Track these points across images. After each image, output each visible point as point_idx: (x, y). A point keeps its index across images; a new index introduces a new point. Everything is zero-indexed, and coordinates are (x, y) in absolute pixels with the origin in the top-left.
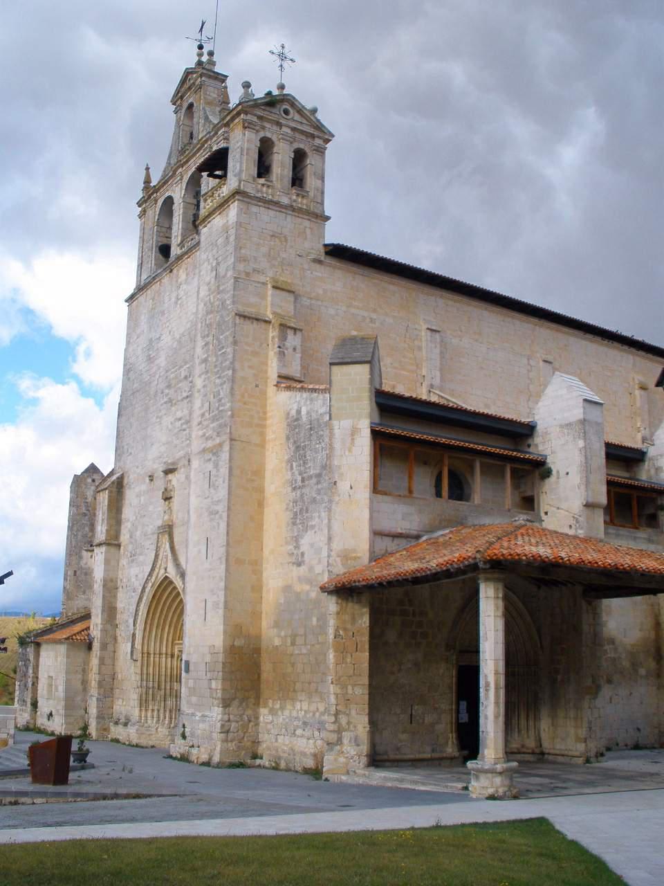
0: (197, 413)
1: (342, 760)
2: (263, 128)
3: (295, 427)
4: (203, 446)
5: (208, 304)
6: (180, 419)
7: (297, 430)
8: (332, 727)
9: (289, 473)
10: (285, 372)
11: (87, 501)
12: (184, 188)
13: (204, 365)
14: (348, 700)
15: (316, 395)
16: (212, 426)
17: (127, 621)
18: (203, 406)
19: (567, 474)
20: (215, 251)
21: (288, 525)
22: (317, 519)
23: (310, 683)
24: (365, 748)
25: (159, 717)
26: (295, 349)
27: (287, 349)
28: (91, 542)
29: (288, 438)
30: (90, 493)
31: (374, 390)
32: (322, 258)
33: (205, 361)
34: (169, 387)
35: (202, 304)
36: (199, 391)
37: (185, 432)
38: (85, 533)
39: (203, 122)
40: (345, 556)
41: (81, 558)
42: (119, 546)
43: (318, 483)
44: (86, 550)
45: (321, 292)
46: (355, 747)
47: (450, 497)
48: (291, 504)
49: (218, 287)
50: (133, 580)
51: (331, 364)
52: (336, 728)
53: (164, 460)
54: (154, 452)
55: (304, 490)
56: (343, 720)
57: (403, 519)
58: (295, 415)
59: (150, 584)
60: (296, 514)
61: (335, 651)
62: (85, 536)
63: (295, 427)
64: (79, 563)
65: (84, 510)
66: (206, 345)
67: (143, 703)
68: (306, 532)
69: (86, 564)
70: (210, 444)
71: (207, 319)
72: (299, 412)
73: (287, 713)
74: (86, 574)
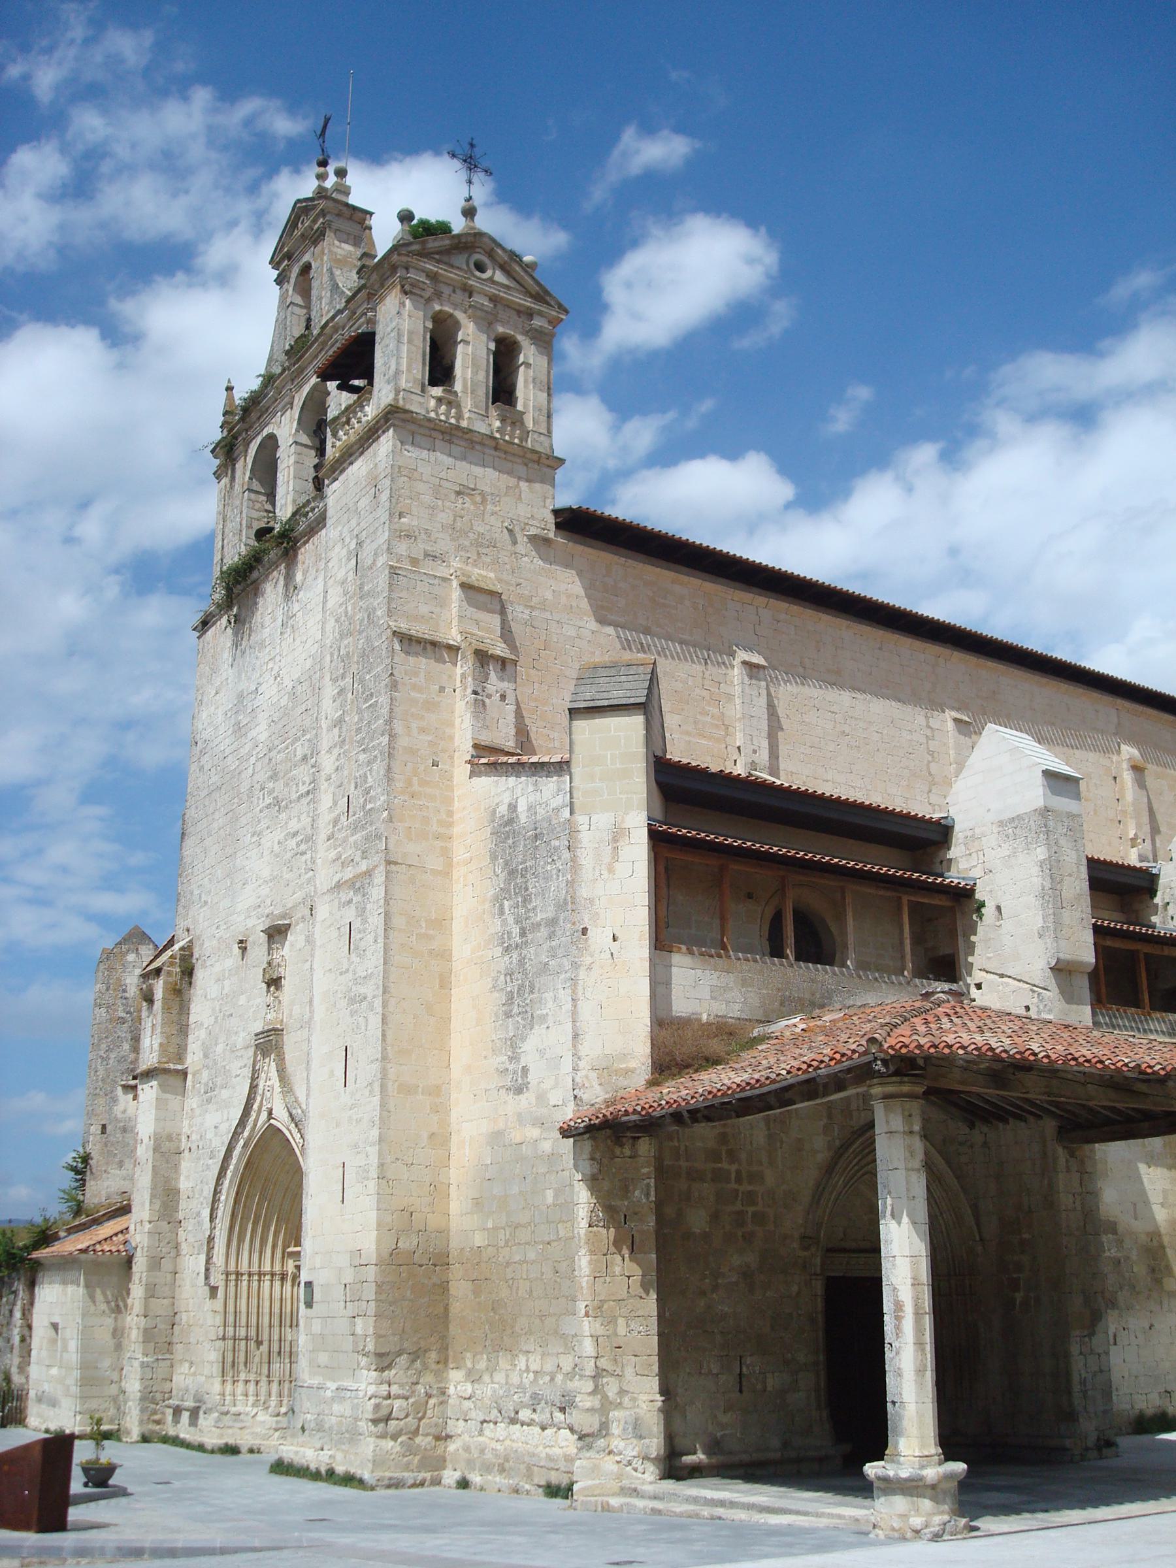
0: (325, 819)
2: (438, 295)
4: (337, 878)
7: (510, 841)
8: (589, 1402)
9: (498, 922)
10: (486, 738)
11: (127, 995)
12: (297, 417)
13: (336, 730)
14: (620, 1347)
16: (352, 839)
17: (198, 1214)
18: (335, 803)
20: (353, 523)
22: (550, 1004)
24: (655, 1445)
26: (503, 697)
27: (489, 696)
29: (494, 857)
31: (652, 760)
32: (551, 535)
33: (339, 722)
34: (274, 777)
35: (333, 620)
36: (328, 779)
37: (304, 858)
39: (328, 294)
40: (606, 1070)
41: (115, 1100)
42: (184, 1073)
45: (549, 595)
46: (635, 1441)
47: (798, 959)
48: (502, 977)
50: (209, 1135)
51: (574, 713)
52: (597, 1404)
53: (267, 911)
54: (247, 898)
55: (524, 952)
56: (612, 1391)
57: (713, 998)
59: (242, 1142)
60: (510, 997)
61: (592, 1252)
66: (340, 693)
67: (228, 1368)
69: (124, 1111)
70: (349, 873)
71: (342, 646)
72: (513, 807)
73: (499, 1377)
74: (124, 1130)
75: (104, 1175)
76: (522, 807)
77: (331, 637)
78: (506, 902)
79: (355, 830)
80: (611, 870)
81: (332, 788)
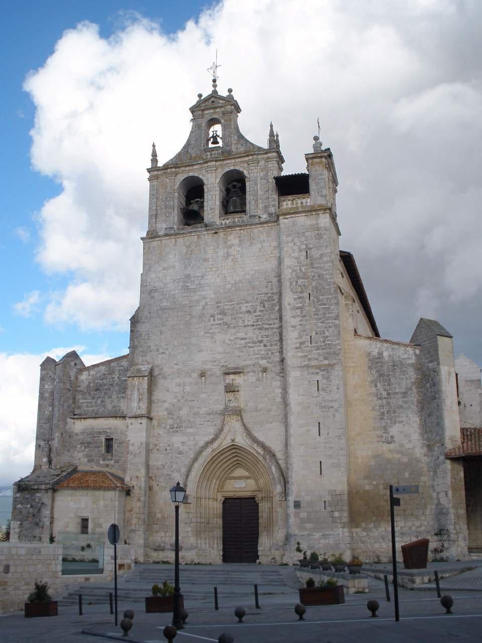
1: (460, 549)
3: (378, 362)
4: (306, 363)
5: (298, 271)
6: (242, 339)
7: (380, 364)
11: (71, 379)
13: (299, 311)
15: (397, 347)
18: (300, 337)
19: (471, 405)
20: (303, 239)
21: (375, 419)
23: (405, 511)
28: (73, 411)
29: (370, 368)
30: (73, 374)
35: (290, 271)
37: (252, 349)
38: (69, 404)
39: (236, 137)
41: (66, 423)
43: (403, 397)
44: (71, 418)
48: (378, 407)
49: (312, 264)
53: (221, 364)
56: (458, 527)
58: (377, 355)
60: (383, 414)
61: (452, 490)
62: (69, 407)
63: (378, 362)
64: (65, 427)
65: (68, 386)
67: (198, 534)
68: (395, 424)
69: (70, 429)
71: (299, 281)
74: (70, 436)
75: (63, 455)
76: (385, 354)
77: (289, 276)
79: (318, 348)
80: (449, 383)
81: (298, 331)
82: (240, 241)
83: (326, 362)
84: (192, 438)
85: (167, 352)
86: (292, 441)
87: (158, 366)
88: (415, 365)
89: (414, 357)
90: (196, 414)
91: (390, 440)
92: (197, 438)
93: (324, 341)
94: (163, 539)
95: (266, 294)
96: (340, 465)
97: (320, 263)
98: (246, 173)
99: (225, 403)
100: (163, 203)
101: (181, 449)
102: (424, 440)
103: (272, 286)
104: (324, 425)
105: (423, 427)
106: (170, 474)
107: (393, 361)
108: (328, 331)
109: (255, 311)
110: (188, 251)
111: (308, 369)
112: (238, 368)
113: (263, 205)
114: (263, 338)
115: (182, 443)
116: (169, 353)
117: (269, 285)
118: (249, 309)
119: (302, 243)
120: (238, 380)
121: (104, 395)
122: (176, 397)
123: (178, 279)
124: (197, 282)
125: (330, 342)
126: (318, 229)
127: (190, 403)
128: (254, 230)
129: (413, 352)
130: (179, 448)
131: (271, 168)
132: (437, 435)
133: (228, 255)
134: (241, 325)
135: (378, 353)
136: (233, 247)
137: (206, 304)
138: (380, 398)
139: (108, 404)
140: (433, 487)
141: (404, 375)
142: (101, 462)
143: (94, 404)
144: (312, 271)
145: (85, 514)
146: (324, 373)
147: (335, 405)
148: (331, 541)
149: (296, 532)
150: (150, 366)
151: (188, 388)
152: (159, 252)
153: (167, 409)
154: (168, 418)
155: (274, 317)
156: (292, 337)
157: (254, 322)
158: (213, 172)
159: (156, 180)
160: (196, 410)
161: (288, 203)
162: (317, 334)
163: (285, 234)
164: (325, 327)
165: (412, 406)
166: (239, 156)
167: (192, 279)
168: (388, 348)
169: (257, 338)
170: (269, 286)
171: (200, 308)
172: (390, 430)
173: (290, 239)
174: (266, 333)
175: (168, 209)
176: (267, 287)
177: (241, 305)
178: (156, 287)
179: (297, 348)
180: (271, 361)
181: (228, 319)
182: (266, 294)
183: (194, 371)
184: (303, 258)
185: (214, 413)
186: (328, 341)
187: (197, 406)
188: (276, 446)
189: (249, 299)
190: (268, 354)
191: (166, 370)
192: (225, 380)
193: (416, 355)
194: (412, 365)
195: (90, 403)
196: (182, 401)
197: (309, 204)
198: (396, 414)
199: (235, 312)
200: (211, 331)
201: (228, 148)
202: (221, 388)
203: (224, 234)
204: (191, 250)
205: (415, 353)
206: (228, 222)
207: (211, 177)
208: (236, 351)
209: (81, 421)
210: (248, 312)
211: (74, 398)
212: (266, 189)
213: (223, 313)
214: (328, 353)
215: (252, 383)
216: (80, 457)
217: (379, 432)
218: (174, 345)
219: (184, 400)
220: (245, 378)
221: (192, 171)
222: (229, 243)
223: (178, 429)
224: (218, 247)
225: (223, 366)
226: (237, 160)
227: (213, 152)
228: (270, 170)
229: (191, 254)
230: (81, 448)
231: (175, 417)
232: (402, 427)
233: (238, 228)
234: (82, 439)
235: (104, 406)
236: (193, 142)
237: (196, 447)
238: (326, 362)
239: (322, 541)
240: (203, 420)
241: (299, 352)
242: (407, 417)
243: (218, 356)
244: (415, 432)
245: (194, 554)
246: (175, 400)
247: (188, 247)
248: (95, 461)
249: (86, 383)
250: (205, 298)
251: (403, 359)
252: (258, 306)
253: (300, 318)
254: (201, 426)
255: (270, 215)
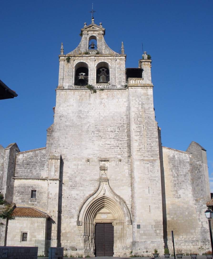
4: (142, 158)
5: (138, 114)
6: (109, 144)
7: (174, 161)
13: (138, 133)
21: (172, 186)
22: (185, 187)
25: (90, 246)
29: (169, 163)
35: (134, 113)
38: (12, 171)
48: (173, 181)
53: (98, 156)
60: (175, 184)
63: (173, 160)
69: (12, 184)
72: (174, 156)
76: (176, 156)
77: (134, 116)
78: (173, 170)
82: (107, 97)
83: (152, 158)
84: (82, 192)
85: (69, 148)
86: (136, 195)
87: (64, 154)
88: (189, 162)
89: (189, 159)
90: (84, 180)
91: (179, 196)
92: (85, 192)
93: (151, 148)
94: (66, 244)
95: (120, 124)
96: (159, 207)
97: (148, 112)
98: (109, 64)
99: (100, 176)
100: (67, 73)
101: (76, 197)
102: (194, 197)
103: (123, 120)
104: (152, 188)
105: (194, 191)
106: (70, 210)
107: (180, 160)
108: (153, 143)
109: (115, 131)
110: (80, 98)
111: (143, 161)
112: (106, 159)
113: (118, 81)
114: (119, 144)
115: (77, 194)
116: (70, 148)
117: (122, 119)
118: (112, 130)
119: (140, 101)
120: (107, 164)
121: (32, 167)
122: (73, 171)
123: (75, 112)
124: (85, 114)
125: (154, 149)
126: (148, 95)
127: (81, 175)
128: (115, 92)
129: (188, 156)
130: (75, 197)
131: (123, 64)
132: (202, 195)
133: (101, 103)
134: (108, 137)
135: (173, 156)
136: (104, 99)
137: (90, 125)
138: (174, 177)
139: (34, 173)
140: (199, 219)
141: (184, 167)
142: (29, 203)
143: (26, 172)
144: (145, 115)
145: (25, 231)
146: (151, 163)
147: (157, 179)
148: (155, 245)
149: (138, 240)
150: (60, 154)
151: (80, 167)
152: (65, 97)
153: (69, 177)
154: (69, 181)
155: (124, 135)
156: (135, 145)
157: (114, 137)
158: (93, 62)
159: (63, 61)
160: (84, 178)
161: (132, 81)
162: (147, 145)
163: (132, 95)
164: (151, 142)
165: (188, 181)
166: (107, 56)
167: (83, 113)
168: (177, 154)
169: (116, 145)
170: (122, 120)
171: (86, 127)
172: (179, 192)
173: (134, 98)
174: (121, 143)
175: (69, 77)
176: (121, 120)
177: (108, 128)
178: (63, 115)
179: (138, 151)
180: (123, 156)
181: (101, 134)
182: (120, 124)
183: (83, 159)
184: (140, 108)
185: (94, 180)
186: (153, 148)
187: (85, 176)
188: (127, 197)
189: (112, 125)
190: (121, 153)
191: (68, 157)
192: (99, 164)
193: (190, 158)
194: (188, 162)
195: (24, 171)
196: (77, 173)
197: (143, 83)
198: (182, 185)
199: (105, 131)
200: (92, 139)
201: (100, 51)
202: (98, 168)
203: (99, 93)
204: (82, 98)
205: (189, 157)
206: (101, 87)
207: (92, 64)
208: (105, 150)
209: (18, 180)
210: (112, 131)
211: (15, 168)
212: (120, 73)
213: (99, 131)
214: (153, 154)
215: (114, 166)
216: (17, 199)
217: (174, 193)
218: (73, 145)
219: (78, 172)
220: (110, 163)
221: (82, 59)
222: (102, 97)
223: (75, 187)
224: (96, 98)
225: (98, 157)
226: (105, 57)
227: (93, 52)
228: (122, 65)
229: (82, 100)
230: (18, 194)
231: (73, 181)
232: (184, 191)
233: (107, 90)
234: (19, 190)
235: (32, 173)
236: (82, 46)
237: (84, 197)
238: (152, 158)
239: (151, 245)
240: (88, 183)
241: (139, 153)
242: (186, 186)
243: (96, 152)
244: (190, 193)
245: (83, 252)
246: (73, 173)
247: (80, 96)
248: (26, 202)
249: (21, 161)
250: (89, 123)
251: (184, 159)
252: (116, 129)
253: (139, 137)
254: (87, 186)
255: (122, 86)
